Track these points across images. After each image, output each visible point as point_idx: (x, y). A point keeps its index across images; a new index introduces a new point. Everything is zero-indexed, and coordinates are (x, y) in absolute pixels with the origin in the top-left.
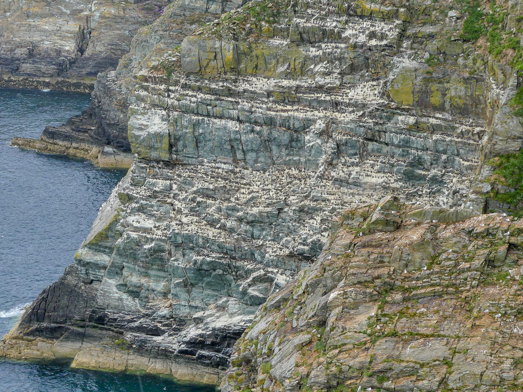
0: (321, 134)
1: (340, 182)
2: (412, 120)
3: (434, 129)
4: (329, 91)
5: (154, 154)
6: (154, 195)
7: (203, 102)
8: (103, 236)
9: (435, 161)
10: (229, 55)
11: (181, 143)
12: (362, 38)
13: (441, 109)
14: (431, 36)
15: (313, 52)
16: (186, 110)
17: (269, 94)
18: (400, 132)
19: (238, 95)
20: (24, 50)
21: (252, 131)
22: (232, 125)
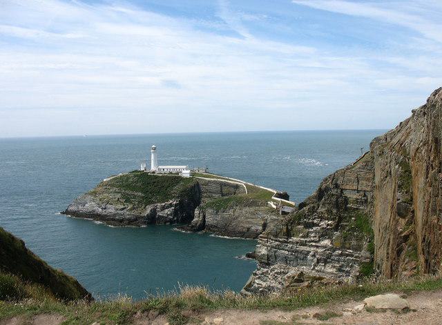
0: (312, 256)
1: (317, 271)
2: (340, 252)
3: (347, 255)
4: (316, 242)
5: (263, 261)
6: (263, 274)
9: (348, 266)
10: (285, 231)
12: (325, 226)
13: (349, 249)
14: (346, 225)
16: (272, 247)
17: (297, 243)
18: (336, 256)
21: (292, 254)
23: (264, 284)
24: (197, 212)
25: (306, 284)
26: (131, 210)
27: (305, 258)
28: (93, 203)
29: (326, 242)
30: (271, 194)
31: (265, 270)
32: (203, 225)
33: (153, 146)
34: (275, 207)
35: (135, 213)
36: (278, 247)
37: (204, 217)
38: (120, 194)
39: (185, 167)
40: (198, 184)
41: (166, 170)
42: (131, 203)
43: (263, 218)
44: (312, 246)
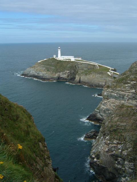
7: (112, 91)
8: (98, 108)
15: (126, 85)
19: (116, 90)
22: (116, 94)
23: (105, 107)
24: (77, 76)
25: (125, 109)
27: (123, 98)
29: (134, 91)
30: (110, 69)
31: (106, 101)
32: (80, 82)
33: (59, 48)
34: (111, 75)
35: (51, 76)
36: (112, 92)
39: (72, 56)
43: (105, 80)
44: (126, 92)
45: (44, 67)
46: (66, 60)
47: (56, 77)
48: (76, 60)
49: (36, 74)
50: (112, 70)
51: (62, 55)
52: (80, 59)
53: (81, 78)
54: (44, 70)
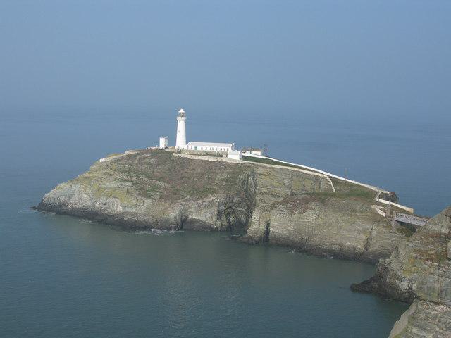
11: (444, 293)
20: (338, 247)
24: (256, 215)
26: (148, 208)
28: (84, 195)
30: (374, 194)
34: (384, 214)
37: (268, 225)
38: (130, 184)
40: (254, 174)
41: (199, 149)
42: (149, 197)
43: (364, 231)
45: (127, 181)
46: (206, 158)
47: (175, 217)
48: (244, 158)
49: (97, 206)
50: (383, 196)
51: (189, 138)
52: (256, 154)
53: (273, 224)
54: (128, 190)
